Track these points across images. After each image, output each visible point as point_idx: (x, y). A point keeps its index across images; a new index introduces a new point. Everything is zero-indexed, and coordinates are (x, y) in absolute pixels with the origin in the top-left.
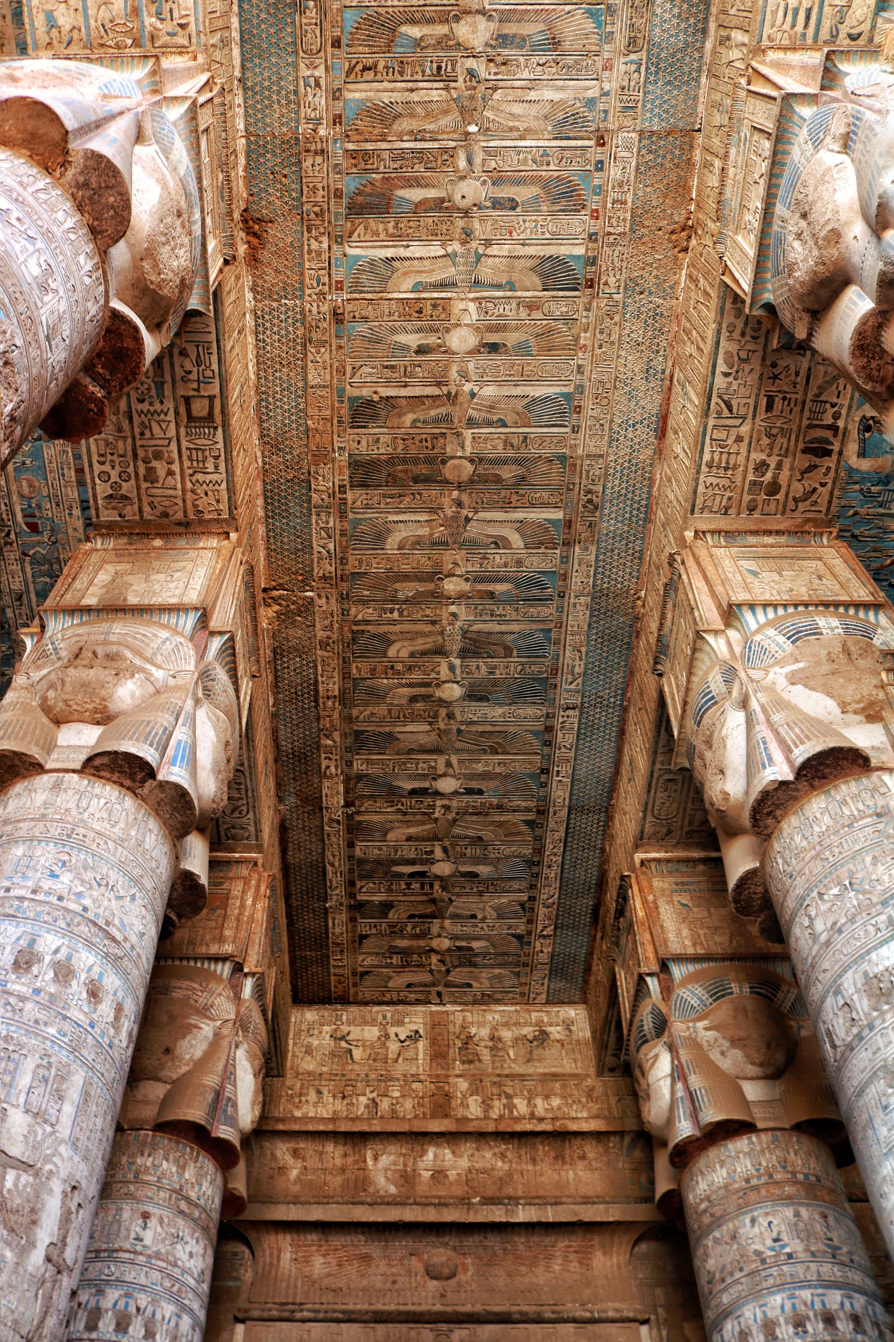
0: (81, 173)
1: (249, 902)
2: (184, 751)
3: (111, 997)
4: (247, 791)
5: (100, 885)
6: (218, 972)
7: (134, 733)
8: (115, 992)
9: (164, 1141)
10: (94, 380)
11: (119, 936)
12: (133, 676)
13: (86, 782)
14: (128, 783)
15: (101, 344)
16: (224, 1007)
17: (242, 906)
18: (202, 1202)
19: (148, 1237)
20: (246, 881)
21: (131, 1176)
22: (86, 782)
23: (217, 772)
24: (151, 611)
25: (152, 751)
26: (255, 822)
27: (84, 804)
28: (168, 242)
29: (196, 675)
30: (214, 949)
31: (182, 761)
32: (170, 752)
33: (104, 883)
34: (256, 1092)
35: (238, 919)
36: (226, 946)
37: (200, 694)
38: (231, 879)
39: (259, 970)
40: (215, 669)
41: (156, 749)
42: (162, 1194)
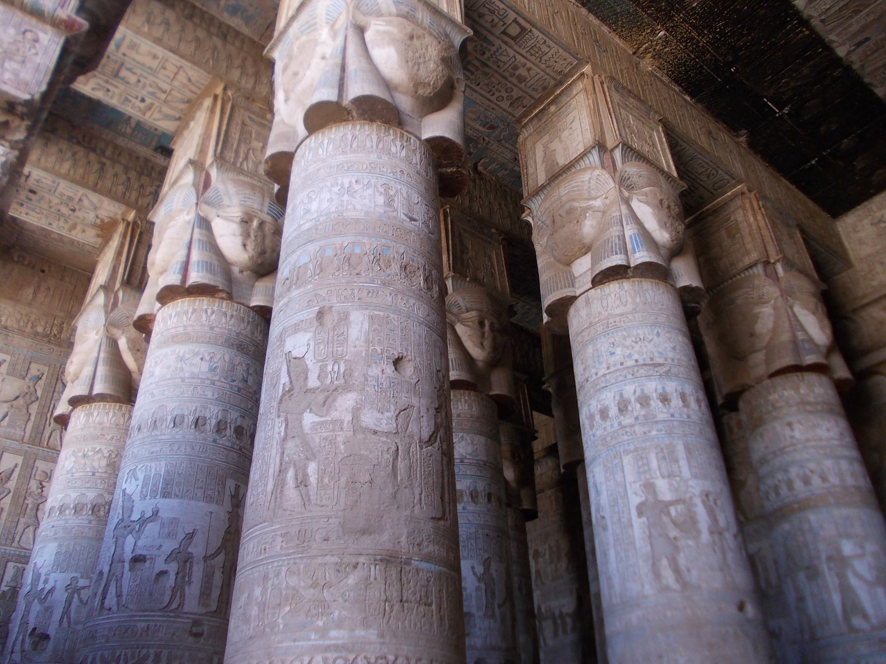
0: (358, 109)
1: (752, 219)
2: (636, 240)
3: (675, 395)
4: (707, 163)
5: (637, 343)
6: (756, 273)
7: (605, 253)
8: (676, 391)
9: (778, 380)
10: (446, 167)
11: (661, 361)
12: (586, 217)
13: (599, 290)
14: (619, 277)
15: (435, 154)
16: (770, 290)
17: (750, 225)
18: (820, 399)
19: (797, 434)
20: (744, 209)
21: (770, 408)
22: (599, 290)
23: (663, 225)
24: (573, 165)
25: (619, 256)
26: (726, 173)
27: (605, 304)
28: (419, 64)
29: (617, 186)
30: (747, 261)
31: (638, 247)
32: (629, 246)
33: (638, 339)
34: (820, 321)
35: (750, 234)
36: (753, 255)
37: (626, 194)
38: (733, 212)
39: (780, 256)
40: (626, 171)
41: (621, 253)
42: (794, 409)
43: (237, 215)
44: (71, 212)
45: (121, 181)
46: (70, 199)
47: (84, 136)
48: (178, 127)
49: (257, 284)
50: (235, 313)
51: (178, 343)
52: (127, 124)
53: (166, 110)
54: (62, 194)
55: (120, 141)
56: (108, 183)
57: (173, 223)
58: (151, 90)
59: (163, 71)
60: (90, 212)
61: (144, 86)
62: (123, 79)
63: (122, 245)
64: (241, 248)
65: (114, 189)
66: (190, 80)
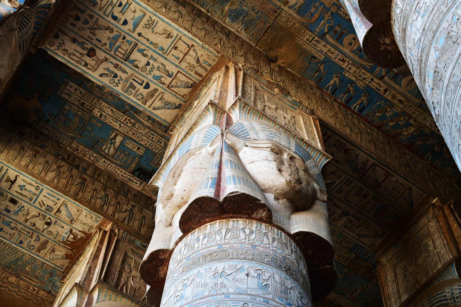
43: (266, 145)
44: (46, 226)
45: (99, 196)
46: (49, 209)
47: (69, 156)
48: (177, 116)
49: (292, 216)
50: (276, 237)
51: (214, 260)
52: (111, 144)
53: (169, 97)
54: (42, 204)
55: (102, 164)
56: (88, 196)
57: (191, 158)
58: (157, 73)
59: (174, 52)
60: (66, 226)
61: (152, 70)
62: (133, 62)
63: (99, 250)
64: (277, 172)
65: (93, 201)
66: (198, 61)
